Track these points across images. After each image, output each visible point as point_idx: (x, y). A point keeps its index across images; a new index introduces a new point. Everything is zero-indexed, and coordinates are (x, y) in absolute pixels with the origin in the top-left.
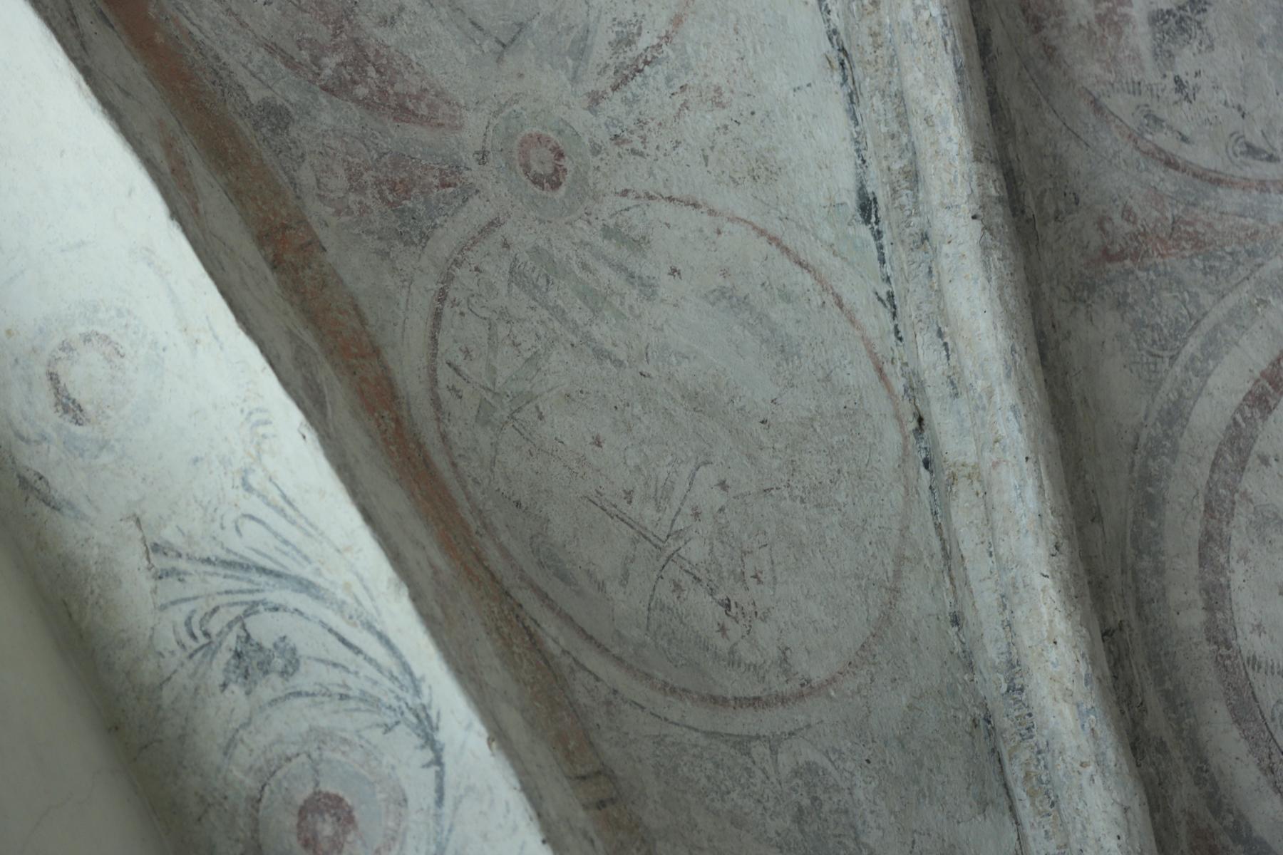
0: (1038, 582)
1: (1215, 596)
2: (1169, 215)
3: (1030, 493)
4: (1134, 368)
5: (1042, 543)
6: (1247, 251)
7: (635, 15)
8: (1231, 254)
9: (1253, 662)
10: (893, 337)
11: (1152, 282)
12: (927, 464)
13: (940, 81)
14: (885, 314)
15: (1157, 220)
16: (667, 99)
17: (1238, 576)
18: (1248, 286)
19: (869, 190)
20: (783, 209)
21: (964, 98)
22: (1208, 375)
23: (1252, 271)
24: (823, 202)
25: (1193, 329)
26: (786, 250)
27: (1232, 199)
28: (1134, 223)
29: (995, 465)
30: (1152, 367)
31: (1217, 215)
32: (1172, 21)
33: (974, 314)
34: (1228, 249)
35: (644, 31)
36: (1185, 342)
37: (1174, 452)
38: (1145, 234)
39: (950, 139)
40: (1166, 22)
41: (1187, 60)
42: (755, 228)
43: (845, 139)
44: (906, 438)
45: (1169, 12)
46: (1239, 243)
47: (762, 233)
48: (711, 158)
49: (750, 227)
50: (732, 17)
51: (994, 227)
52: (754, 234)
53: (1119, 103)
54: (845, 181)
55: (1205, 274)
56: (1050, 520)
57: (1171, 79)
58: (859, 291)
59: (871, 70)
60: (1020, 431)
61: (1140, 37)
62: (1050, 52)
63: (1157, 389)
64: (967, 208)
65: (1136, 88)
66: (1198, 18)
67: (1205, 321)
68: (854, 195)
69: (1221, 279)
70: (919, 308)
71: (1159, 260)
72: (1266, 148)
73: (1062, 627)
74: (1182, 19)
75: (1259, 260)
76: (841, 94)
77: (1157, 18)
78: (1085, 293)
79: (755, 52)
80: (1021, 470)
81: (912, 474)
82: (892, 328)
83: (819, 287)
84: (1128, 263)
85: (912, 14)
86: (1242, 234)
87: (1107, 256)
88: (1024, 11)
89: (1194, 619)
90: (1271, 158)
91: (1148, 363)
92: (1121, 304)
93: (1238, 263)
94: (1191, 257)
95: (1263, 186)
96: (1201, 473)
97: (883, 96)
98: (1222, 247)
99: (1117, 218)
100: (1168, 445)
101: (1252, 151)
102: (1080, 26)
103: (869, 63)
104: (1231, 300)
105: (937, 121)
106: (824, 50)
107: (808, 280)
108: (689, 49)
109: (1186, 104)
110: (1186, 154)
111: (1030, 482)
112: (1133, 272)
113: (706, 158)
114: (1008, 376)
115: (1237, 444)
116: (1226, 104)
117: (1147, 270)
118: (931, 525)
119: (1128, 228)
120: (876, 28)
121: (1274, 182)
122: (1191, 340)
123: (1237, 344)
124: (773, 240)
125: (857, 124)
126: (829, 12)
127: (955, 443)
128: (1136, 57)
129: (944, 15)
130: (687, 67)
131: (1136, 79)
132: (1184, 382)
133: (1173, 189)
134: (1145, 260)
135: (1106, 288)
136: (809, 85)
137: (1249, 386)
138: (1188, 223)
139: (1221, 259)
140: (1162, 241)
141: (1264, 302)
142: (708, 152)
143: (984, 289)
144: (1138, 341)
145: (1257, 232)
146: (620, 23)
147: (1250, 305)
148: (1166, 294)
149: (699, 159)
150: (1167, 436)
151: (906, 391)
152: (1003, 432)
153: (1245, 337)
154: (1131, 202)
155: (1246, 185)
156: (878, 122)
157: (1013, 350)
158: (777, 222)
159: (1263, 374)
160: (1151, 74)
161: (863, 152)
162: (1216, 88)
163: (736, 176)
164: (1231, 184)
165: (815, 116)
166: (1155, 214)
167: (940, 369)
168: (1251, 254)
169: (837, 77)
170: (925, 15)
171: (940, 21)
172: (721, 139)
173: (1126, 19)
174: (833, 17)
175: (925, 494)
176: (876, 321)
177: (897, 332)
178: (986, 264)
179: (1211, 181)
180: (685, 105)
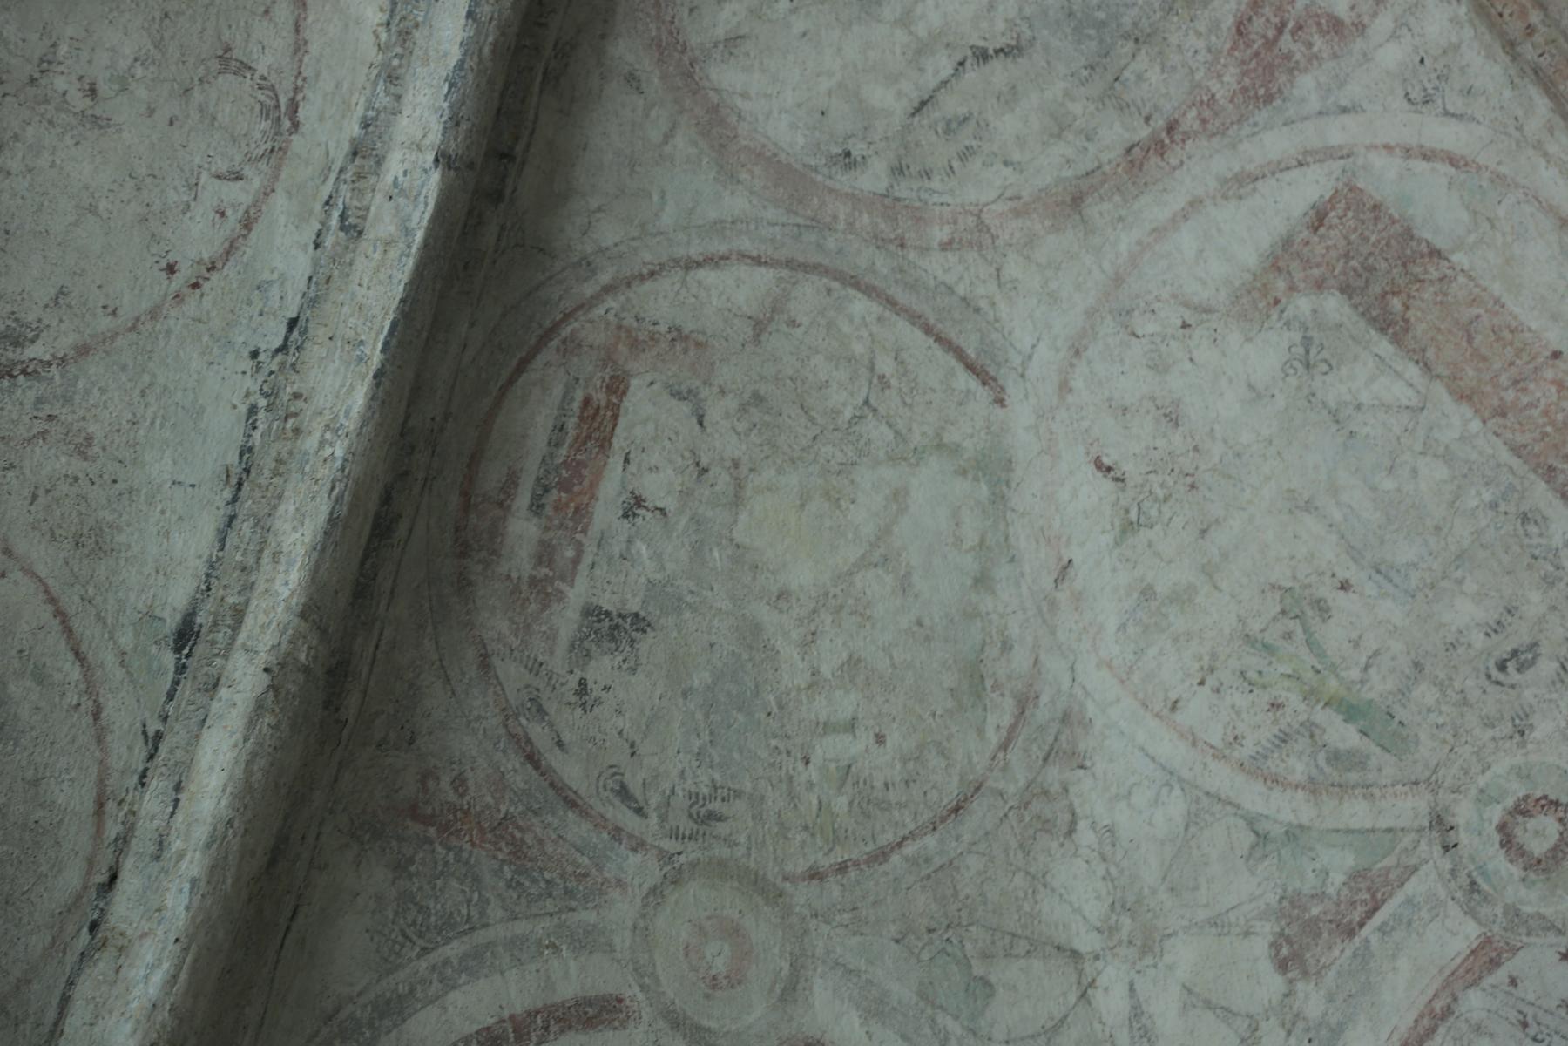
2: (503, 809)
3: (158, 978)
4: (376, 939)
5: (139, 1035)
6: (565, 888)
7: (39, 321)
8: (548, 882)
10: (135, 778)
11: (446, 864)
12: (94, 927)
13: (307, 521)
14: (140, 752)
15: (488, 806)
16: (26, 419)
18: (546, 923)
19: (199, 620)
20: (91, 591)
21: (323, 550)
22: (454, 988)
23: (560, 911)
24: (140, 606)
25: (465, 933)
26: (68, 631)
27: (578, 829)
28: (461, 796)
29: (144, 935)
30: (397, 947)
31: (554, 836)
32: (607, 623)
33: (212, 768)
34: (547, 875)
35: (39, 342)
36: (448, 941)
38: (466, 813)
39: (287, 583)
40: (599, 621)
41: (602, 669)
42: (47, 591)
43: (200, 557)
44: (85, 887)
45: (607, 613)
46: (562, 876)
47: (52, 600)
48: (41, 500)
49: (42, 588)
50: (146, 378)
51: (283, 692)
52: (42, 596)
53: (510, 672)
54: (178, 596)
55: (509, 887)
56: (163, 1015)
57: (577, 678)
58: (126, 713)
59: (258, 494)
60: (188, 908)
61: (566, 620)
62: (464, 584)
63: (389, 972)
64: (263, 658)
65: (536, 667)
66: (634, 634)
67: (482, 932)
68: (179, 617)
69: (523, 900)
70: (171, 751)
71: (467, 846)
72: (640, 799)
74: (617, 627)
75: (573, 904)
76: (222, 512)
77: (593, 613)
78: (367, 837)
79: (152, 423)
80: (164, 949)
81: (71, 928)
82: (141, 768)
83: (83, 687)
84: (432, 831)
85: (316, 445)
86: (570, 869)
87: (414, 812)
88: (457, 530)
90: (639, 811)
91: (395, 942)
92: (400, 868)
93: (550, 895)
94: (503, 861)
95: (617, 833)
97: (256, 525)
98: (541, 870)
99: (445, 781)
100: (368, 1034)
101: (624, 793)
102: (509, 577)
103: (260, 486)
104: (521, 927)
105: (283, 559)
106: (229, 461)
107: (76, 674)
108: (80, 384)
109: (579, 711)
110: (554, 759)
111: (166, 966)
112: (432, 843)
113: (35, 497)
114: (208, 846)
116: (620, 733)
117: (449, 849)
118: (58, 993)
119: (452, 797)
120: (284, 455)
121: (631, 836)
122: (455, 943)
123: (502, 973)
124: (61, 614)
125: (222, 549)
126: (254, 428)
127: (123, 908)
128: (551, 636)
129: (345, 460)
130: (67, 400)
131: (540, 658)
132: (423, 981)
133: (522, 785)
134: (453, 838)
135: (394, 843)
136: (193, 486)
137: (491, 1021)
138: (518, 827)
139: (534, 881)
140: (481, 829)
141: (552, 946)
142: (41, 492)
143: (235, 746)
144: (396, 913)
145: (586, 875)
146: (16, 320)
147: (539, 943)
148: (454, 884)
149: (26, 493)
150: (371, 1025)
151: (116, 840)
152: (169, 903)
153: (514, 971)
154: (469, 774)
155: (600, 823)
156: (237, 548)
157: (230, 823)
158: (76, 599)
159: (512, 1017)
160: (558, 662)
161: (213, 580)
162: (619, 712)
163: (58, 532)
165: (180, 518)
166: (489, 799)
167: (156, 823)
168: (569, 893)
169: (228, 494)
170: (328, 451)
171: (338, 464)
172: (64, 488)
173: (561, 596)
174: (257, 435)
175: (71, 958)
176: (126, 752)
177: (144, 775)
178: (251, 723)
179: (565, 799)
180: (43, 435)
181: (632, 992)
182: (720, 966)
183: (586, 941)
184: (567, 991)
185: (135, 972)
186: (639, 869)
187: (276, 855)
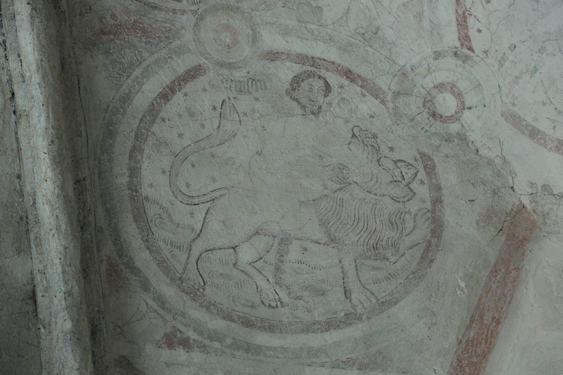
0: (42, 156)
1: (134, 172)
2: (132, 19)
3: (43, 119)
4: (110, 79)
5: (46, 140)
6: (165, 37)
8: (158, 37)
9: (147, 198)
10: (4, 59)
11: (122, 45)
12: (15, 112)
15: (127, 20)
17: (145, 164)
18: (165, 51)
22: (143, 84)
23: (167, 45)
25: (138, 65)
27: (160, 15)
28: (116, 20)
29: (31, 108)
30: (118, 79)
31: (154, 21)
33: (26, 44)
34: (157, 35)
36: (134, 70)
37: (124, 114)
38: (120, 25)
44: (6, 101)
46: (162, 33)
51: (38, 9)
55: (146, 44)
56: (51, 130)
60: (41, 93)
63: (119, 88)
67: (144, 63)
69: (153, 47)
70: (11, 45)
71: (126, 36)
73: (50, 174)
75: (170, 41)
78: (91, 47)
80: (40, 110)
81: (7, 116)
82: (4, 55)
84: (112, 36)
86: (164, 30)
87: (102, 32)
89: (124, 180)
91: (117, 77)
92: (107, 53)
93: (161, 41)
94: (140, 36)
95: (174, 11)
96: (135, 123)
98: (155, 34)
99: (108, 18)
100: (122, 110)
104: (156, 56)
111: (43, 115)
112: (113, 40)
114: (38, 71)
115: (152, 113)
117: (120, 40)
118: (14, 138)
119: (113, 22)
121: (179, 10)
122: (137, 70)
123: (157, 73)
127: (20, 102)
132: (132, 86)
133: (135, 8)
134: (120, 36)
135: (101, 45)
137: (160, 90)
138: (140, 23)
139: (154, 39)
140: (128, 29)
141: (171, 58)
143: (31, 34)
144: (113, 68)
145: (170, 30)
147: (165, 58)
148: (127, 50)
150: (122, 107)
151: (8, 81)
152: (34, 94)
153: (161, 70)
154: (115, 12)
155: (167, 10)
157: (41, 60)
159: (167, 86)
164: (161, 9)
166: (126, 18)
167: (18, 71)
168: (167, 38)
175: (13, 125)
177: (6, 56)
178: (32, 24)
179: (152, 7)
181: (203, 61)
182: (228, 40)
183: (180, 51)
184: (181, 70)
185: (34, 121)
186: (187, 20)
187: (63, 65)
